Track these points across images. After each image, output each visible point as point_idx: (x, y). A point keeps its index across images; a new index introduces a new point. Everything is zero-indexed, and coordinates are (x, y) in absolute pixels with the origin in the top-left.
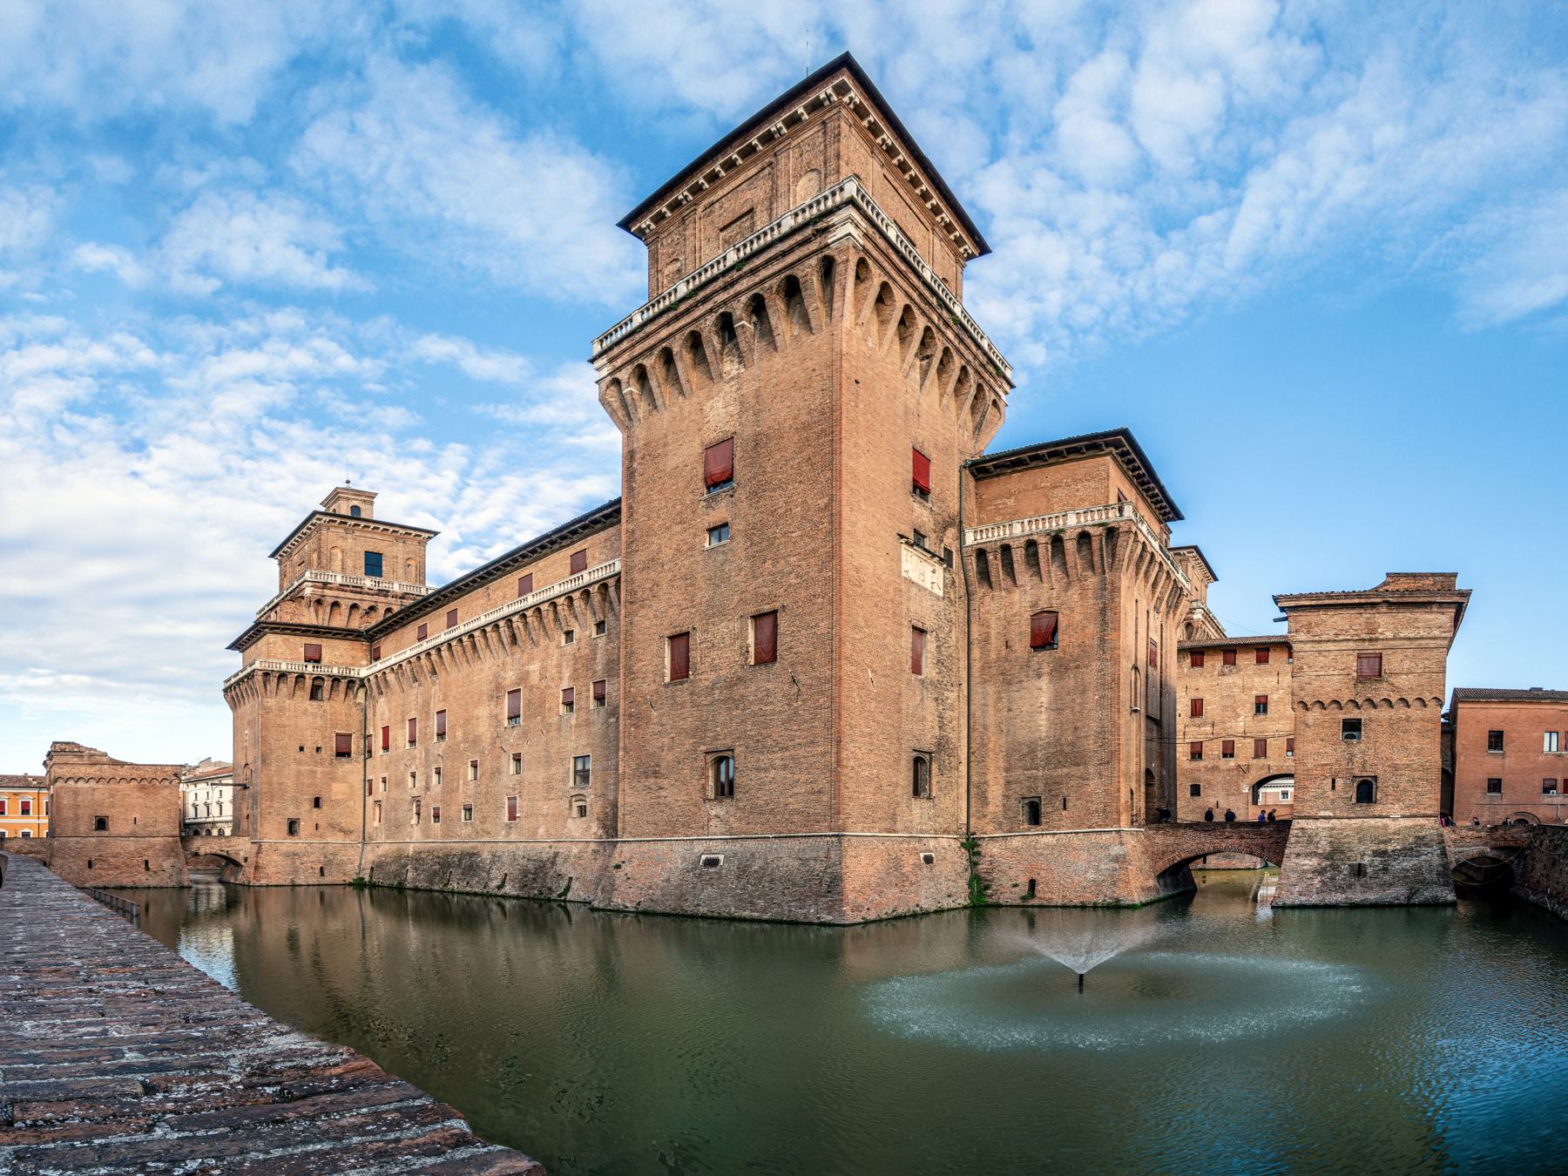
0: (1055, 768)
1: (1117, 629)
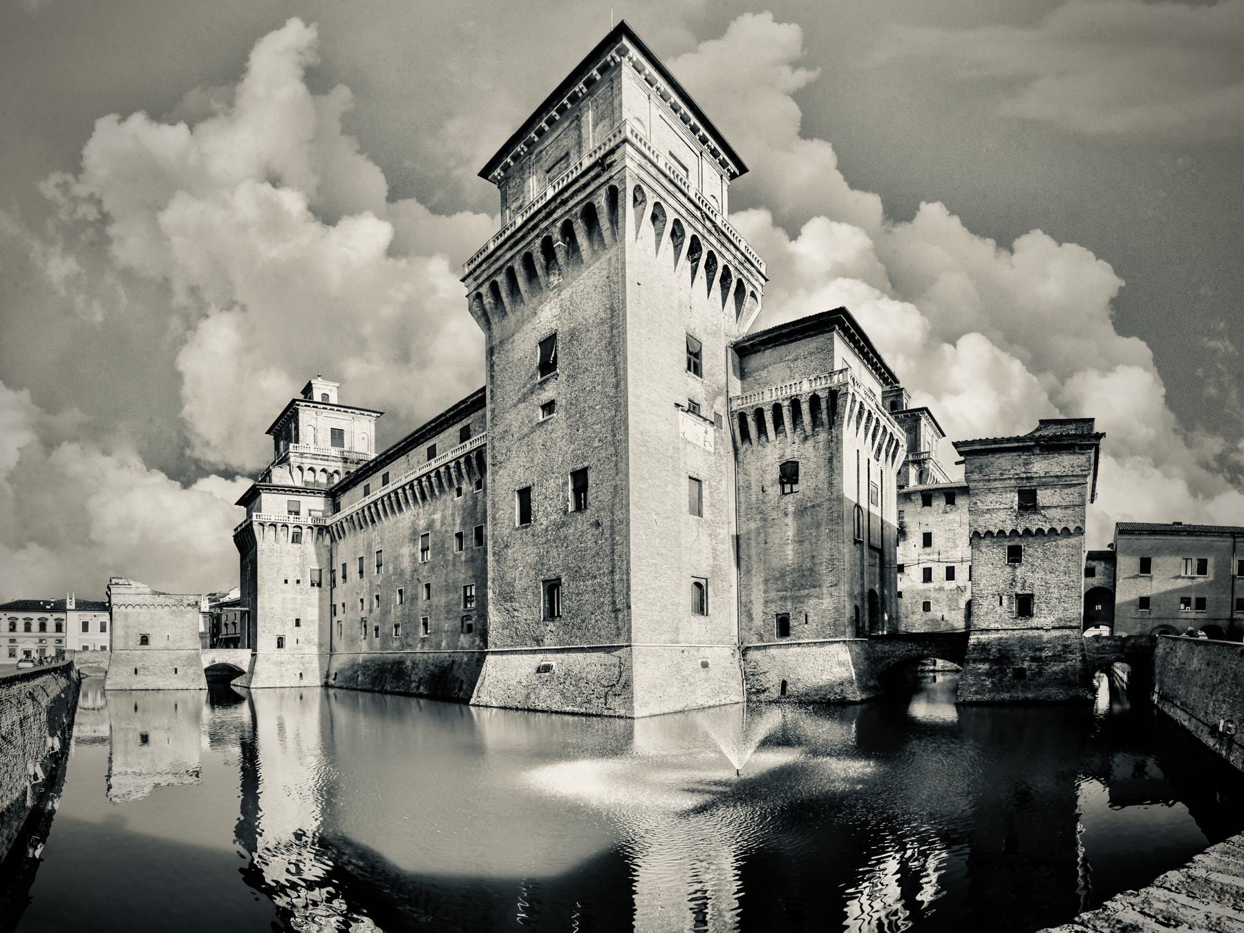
0: (799, 589)
1: (841, 475)
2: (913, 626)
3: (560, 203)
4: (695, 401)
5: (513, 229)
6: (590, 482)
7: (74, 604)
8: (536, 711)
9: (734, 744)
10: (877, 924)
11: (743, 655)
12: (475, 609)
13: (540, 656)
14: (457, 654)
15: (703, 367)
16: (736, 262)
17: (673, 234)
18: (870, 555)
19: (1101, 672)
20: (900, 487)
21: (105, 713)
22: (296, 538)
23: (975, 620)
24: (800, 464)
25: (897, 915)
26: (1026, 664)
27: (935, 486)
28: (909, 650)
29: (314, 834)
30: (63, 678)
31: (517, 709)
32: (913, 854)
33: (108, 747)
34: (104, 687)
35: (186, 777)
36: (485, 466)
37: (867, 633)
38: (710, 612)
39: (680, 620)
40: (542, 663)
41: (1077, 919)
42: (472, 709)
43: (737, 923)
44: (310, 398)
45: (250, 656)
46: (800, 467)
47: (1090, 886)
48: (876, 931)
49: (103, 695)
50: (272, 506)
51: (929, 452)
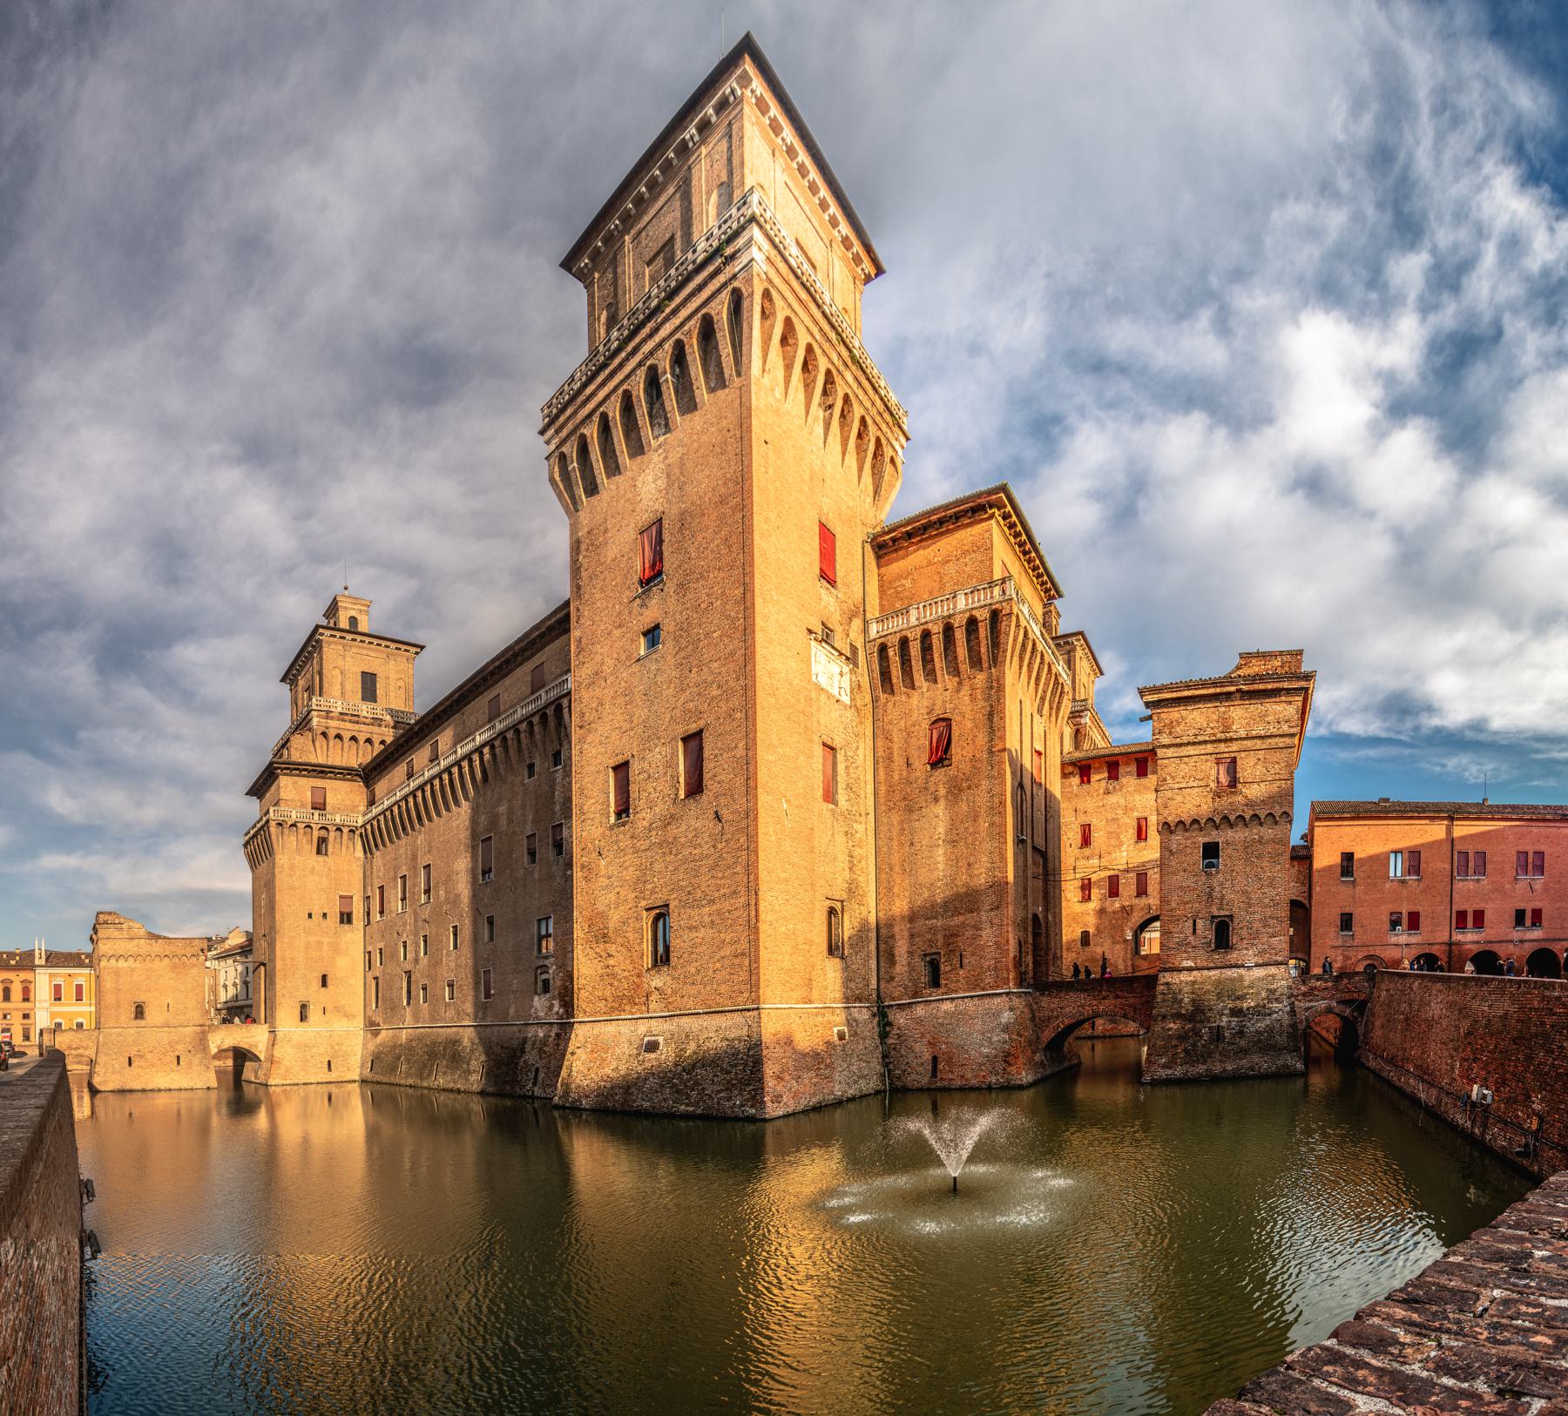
24: (953, 723)
46: (954, 727)
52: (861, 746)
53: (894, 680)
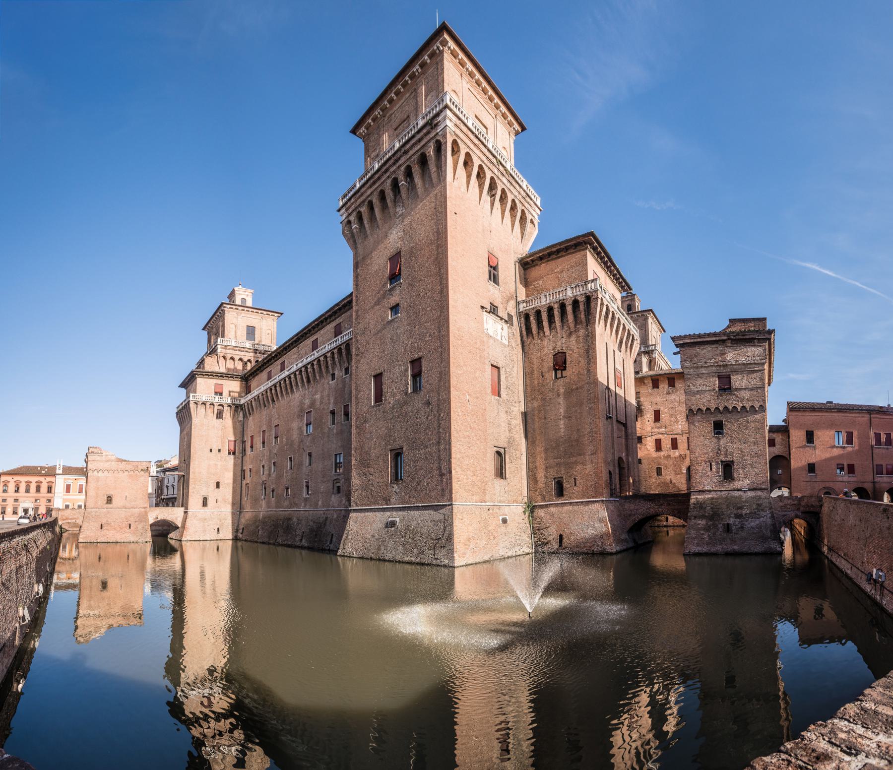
0: (569, 457)
1: (595, 363)
2: (650, 488)
3: (404, 153)
4: (495, 304)
5: (372, 172)
6: (423, 369)
7: (61, 470)
8: (384, 560)
9: (527, 590)
10: (636, 753)
11: (532, 512)
12: (342, 474)
13: (388, 514)
14: (329, 512)
15: (500, 278)
16: (520, 197)
17: (478, 175)
18: (619, 429)
19: (785, 527)
20: (637, 373)
21: (77, 562)
22: (220, 415)
23: (694, 483)
24: (567, 355)
25: (650, 745)
26: (732, 521)
27: (660, 372)
28: (649, 509)
29: (222, 670)
30: (49, 532)
31: (371, 559)
32: (659, 688)
33: (77, 592)
34: (78, 540)
35: (132, 619)
36: (351, 355)
37: (619, 494)
38: (507, 476)
39: (487, 482)
40: (390, 519)
41: (782, 748)
42: (339, 559)
43: (532, 752)
44: (233, 302)
45: (183, 514)
46: (567, 357)
47: (790, 718)
48: (635, 759)
49: (77, 547)
50: (204, 388)
51: (655, 345)
52: (516, 366)
53: (534, 333)
